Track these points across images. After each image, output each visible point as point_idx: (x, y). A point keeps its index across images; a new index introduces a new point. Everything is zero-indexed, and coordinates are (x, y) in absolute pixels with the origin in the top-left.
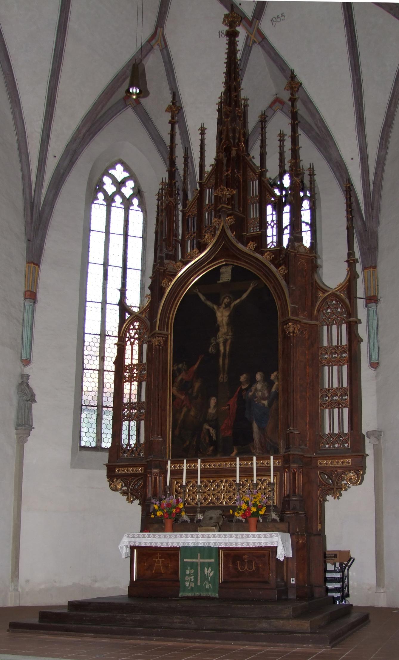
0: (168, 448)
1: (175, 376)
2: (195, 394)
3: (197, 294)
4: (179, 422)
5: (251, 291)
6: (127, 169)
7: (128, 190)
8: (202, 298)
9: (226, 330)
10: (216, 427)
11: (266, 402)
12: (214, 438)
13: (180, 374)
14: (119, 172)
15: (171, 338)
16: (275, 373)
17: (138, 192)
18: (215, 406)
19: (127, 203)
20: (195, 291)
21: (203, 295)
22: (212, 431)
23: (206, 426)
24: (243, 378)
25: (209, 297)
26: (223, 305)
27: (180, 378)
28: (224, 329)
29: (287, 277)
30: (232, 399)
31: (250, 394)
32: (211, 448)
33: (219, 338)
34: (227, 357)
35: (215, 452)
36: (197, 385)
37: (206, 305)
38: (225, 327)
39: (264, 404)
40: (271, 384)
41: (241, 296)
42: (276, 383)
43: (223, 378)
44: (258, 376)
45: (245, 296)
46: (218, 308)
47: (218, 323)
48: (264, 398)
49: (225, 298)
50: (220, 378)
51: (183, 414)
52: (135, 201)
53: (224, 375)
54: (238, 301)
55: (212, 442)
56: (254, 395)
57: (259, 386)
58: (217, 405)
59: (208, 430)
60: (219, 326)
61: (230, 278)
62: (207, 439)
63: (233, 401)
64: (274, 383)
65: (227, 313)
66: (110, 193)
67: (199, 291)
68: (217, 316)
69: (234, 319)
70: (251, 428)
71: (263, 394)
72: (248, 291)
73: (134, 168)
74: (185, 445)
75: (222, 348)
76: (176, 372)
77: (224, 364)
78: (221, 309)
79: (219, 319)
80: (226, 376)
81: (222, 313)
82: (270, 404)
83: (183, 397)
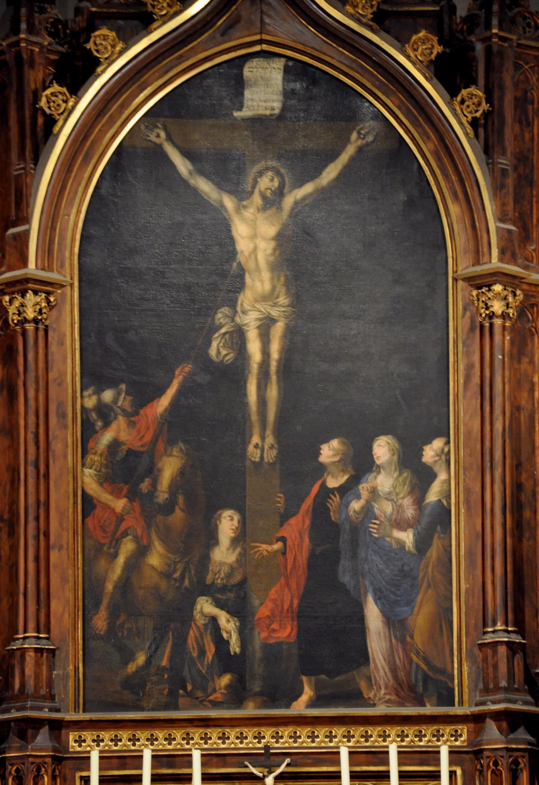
2: (162, 496)
3: (160, 147)
4: (110, 587)
9: (267, 286)
10: (240, 610)
11: (407, 537)
12: (235, 647)
13: (107, 425)
16: (438, 443)
18: (235, 542)
20: (153, 138)
22: (228, 624)
23: (205, 606)
24: (329, 452)
26: (257, 199)
27: (107, 438)
28: (260, 282)
31: (356, 505)
32: (225, 680)
33: (244, 312)
34: (274, 378)
35: (237, 695)
36: (169, 468)
38: (266, 275)
39: (401, 544)
40: (423, 477)
41: (317, 172)
42: (442, 476)
44: (383, 449)
45: (331, 173)
46: (238, 209)
47: (240, 258)
48: (401, 525)
49: (261, 174)
50: (251, 448)
51: (121, 560)
53: (263, 438)
54: (308, 188)
55: (226, 661)
56: (368, 512)
57: (384, 482)
58: (240, 538)
59: (214, 619)
60: (241, 274)
61: (277, 106)
62: (211, 650)
63: (298, 528)
64: (433, 476)
65: (270, 230)
67: (169, 138)
68: (235, 234)
69: (295, 255)
70: (361, 619)
71: (399, 508)
72: (344, 158)
74: (132, 668)
75: (254, 347)
76: (94, 415)
77: (262, 402)
78: (249, 213)
79: (243, 245)
80: (270, 440)
81: (253, 224)
82: (423, 544)
83: (120, 504)
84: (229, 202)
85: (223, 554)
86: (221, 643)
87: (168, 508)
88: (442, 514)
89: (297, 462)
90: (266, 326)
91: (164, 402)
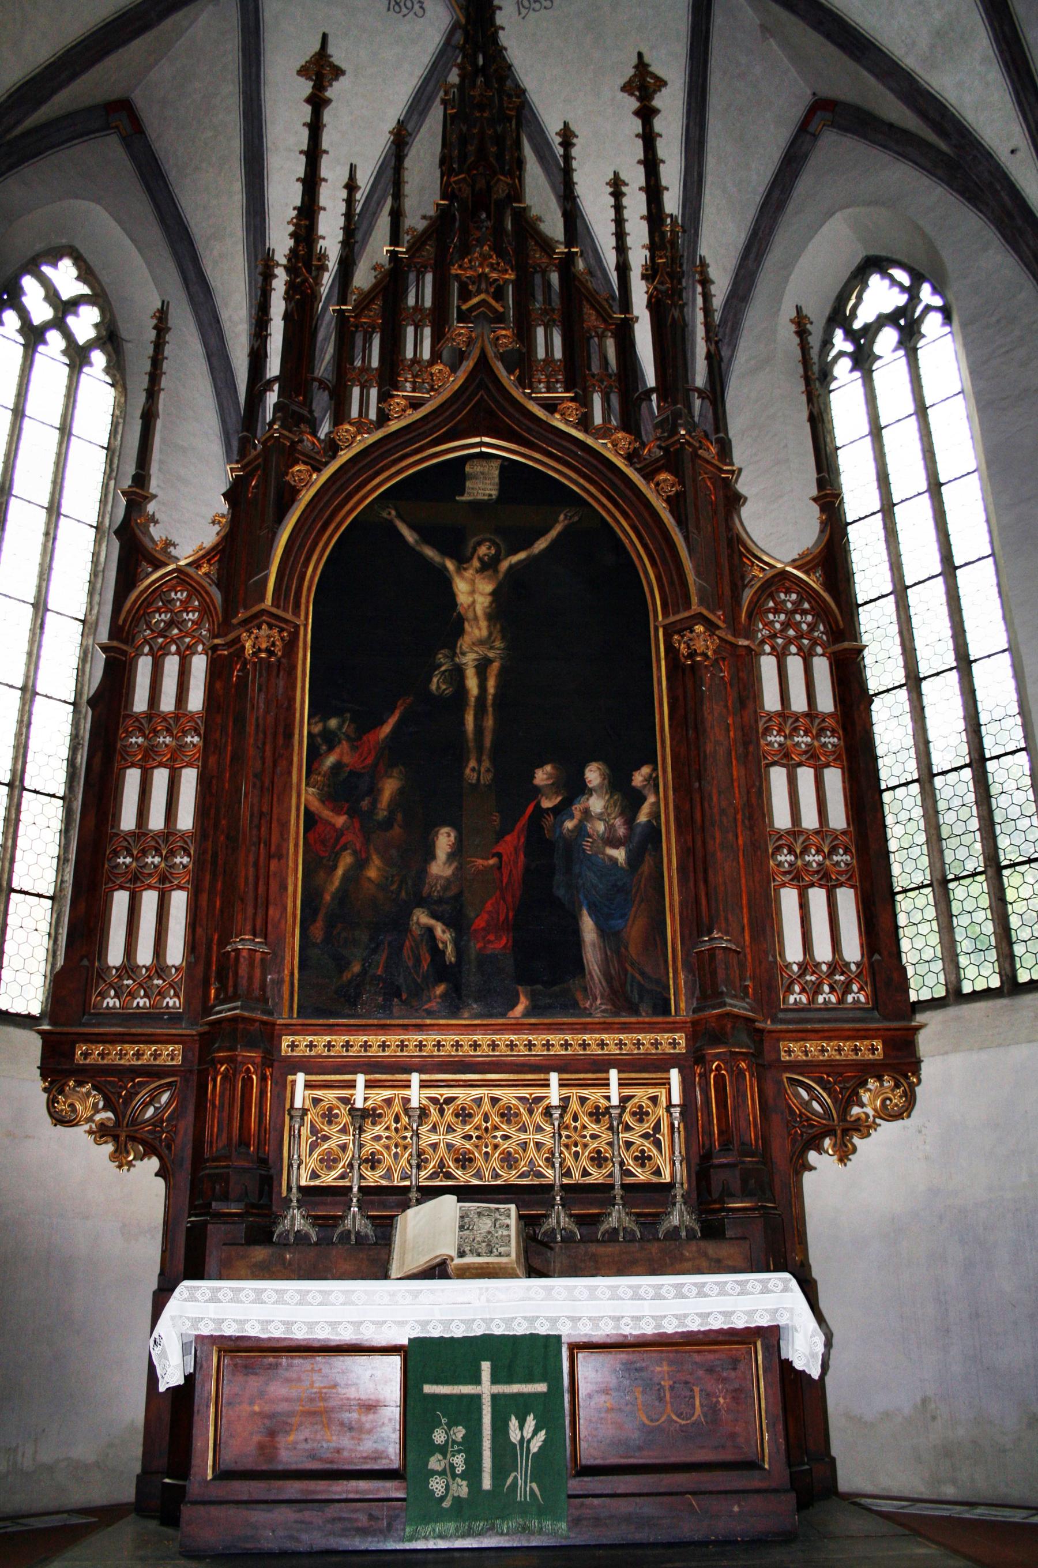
0: (287, 979)
1: (314, 755)
2: (382, 814)
3: (391, 522)
4: (328, 898)
5: (559, 535)
6: (86, 274)
7: (85, 324)
8: (409, 536)
9: (485, 633)
10: (456, 922)
11: (619, 854)
13: (331, 749)
14: (65, 278)
15: (306, 636)
16: (646, 770)
17: (109, 337)
18: (451, 857)
19: (77, 357)
20: (385, 515)
21: (412, 527)
23: (422, 917)
24: (542, 776)
25: (427, 535)
26: (476, 563)
27: (331, 760)
28: (477, 630)
29: (675, 503)
30: (508, 838)
31: (569, 825)
32: (440, 989)
33: (464, 654)
34: (490, 709)
36: (389, 787)
37: (421, 556)
38: (483, 624)
39: (614, 861)
41: (528, 544)
42: (651, 799)
43: (476, 770)
44: (593, 775)
46: (459, 570)
47: (460, 608)
48: (614, 842)
49: (479, 544)
50: (468, 771)
51: (340, 872)
52: (98, 358)
53: (479, 761)
54: (522, 556)
55: (442, 971)
56: (581, 830)
57: (596, 804)
58: (456, 853)
59: (430, 930)
60: (461, 620)
61: (495, 493)
63: (512, 844)
64: (644, 799)
65: (486, 587)
66: (36, 322)
67: (399, 516)
68: (456, 590)
71: (610, 828)
72: (553, 533)
73: (105, 278)
74: (347, 976)
75: (472, 683)
76: (319, 740)
77: (479, 729)
78: (469, 574)
80: (486, 764)
81: (472, 582)
82: (635, 859)
83: (340, 821)
84: (450, 565)
85: (440, 868)
86: (437, 953)
87: (388, 824)
88: (653, 834)
89: (512, 787)
90: (482, 667)
91: (386, 729)
